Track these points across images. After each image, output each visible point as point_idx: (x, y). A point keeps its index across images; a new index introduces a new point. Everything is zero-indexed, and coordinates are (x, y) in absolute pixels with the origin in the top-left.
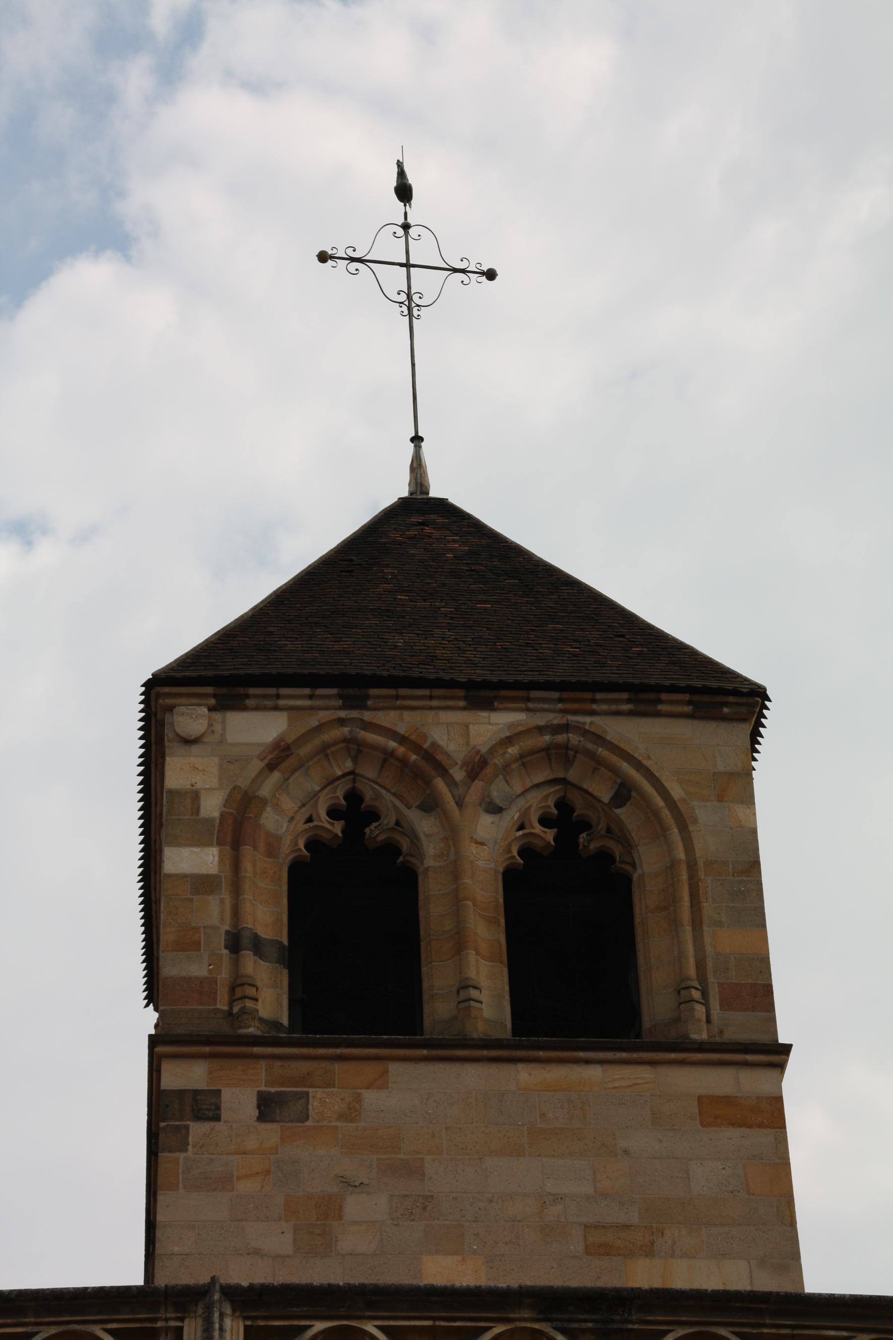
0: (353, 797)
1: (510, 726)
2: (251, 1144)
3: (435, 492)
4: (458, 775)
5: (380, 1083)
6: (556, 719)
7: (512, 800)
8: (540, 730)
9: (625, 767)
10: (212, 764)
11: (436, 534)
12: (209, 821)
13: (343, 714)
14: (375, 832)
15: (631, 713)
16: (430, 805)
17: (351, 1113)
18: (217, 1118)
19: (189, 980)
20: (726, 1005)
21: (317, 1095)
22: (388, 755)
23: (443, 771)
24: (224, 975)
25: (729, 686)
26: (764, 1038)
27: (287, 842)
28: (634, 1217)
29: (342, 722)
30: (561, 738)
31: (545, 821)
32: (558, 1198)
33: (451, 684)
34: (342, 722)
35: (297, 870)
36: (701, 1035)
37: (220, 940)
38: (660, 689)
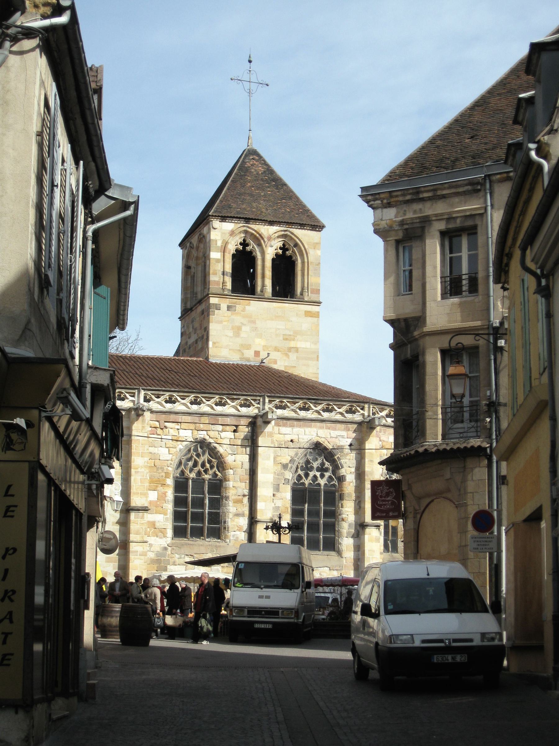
0: (244, 240)
1: (276, 230)
2: (226, 315)
3: (255, 147)
4: (266, 240)
5: (249, 305)
6: (286, 229)
7: (274, 244)
8: (282, 231)
9: (297, 240)
10: (219, 234)
11: (257, 163)
12: (219, 247)
13: (244, 225)
14: (248, 249)
15: (299, 229)
16: (259, 245)
17: (244, 310)
18: (220, 310)
19: (215, 281)
20: (311, 293)
21: (237, 306)
22: (252, 234)
23: (263, 239)
24: (222, 280)
25: (319, 225)
26: (317, 300)
27: (232, 250)
28: (292, 334)
29: (244, 226)
30: (286, 233)
31: (280, 248)
32: (279, 329)
33: (267, 221)
34: (244, 226)
35: (234, 256)
36: (306, 299)
37: (221, 273)
38: (305, 224)
